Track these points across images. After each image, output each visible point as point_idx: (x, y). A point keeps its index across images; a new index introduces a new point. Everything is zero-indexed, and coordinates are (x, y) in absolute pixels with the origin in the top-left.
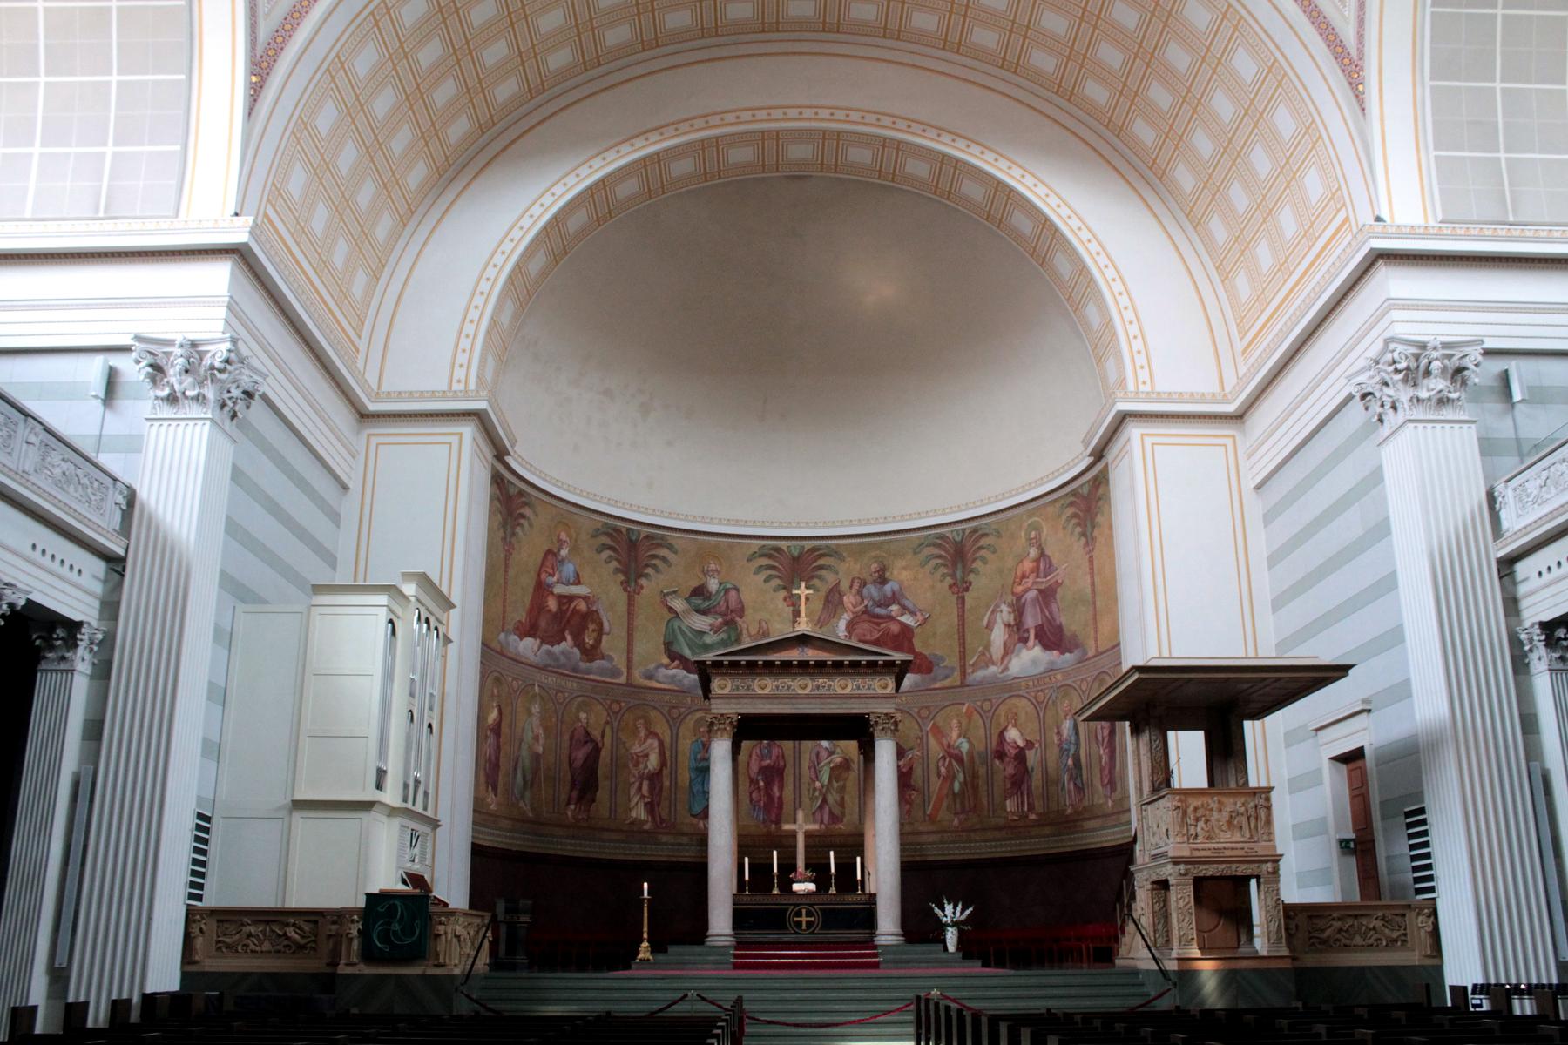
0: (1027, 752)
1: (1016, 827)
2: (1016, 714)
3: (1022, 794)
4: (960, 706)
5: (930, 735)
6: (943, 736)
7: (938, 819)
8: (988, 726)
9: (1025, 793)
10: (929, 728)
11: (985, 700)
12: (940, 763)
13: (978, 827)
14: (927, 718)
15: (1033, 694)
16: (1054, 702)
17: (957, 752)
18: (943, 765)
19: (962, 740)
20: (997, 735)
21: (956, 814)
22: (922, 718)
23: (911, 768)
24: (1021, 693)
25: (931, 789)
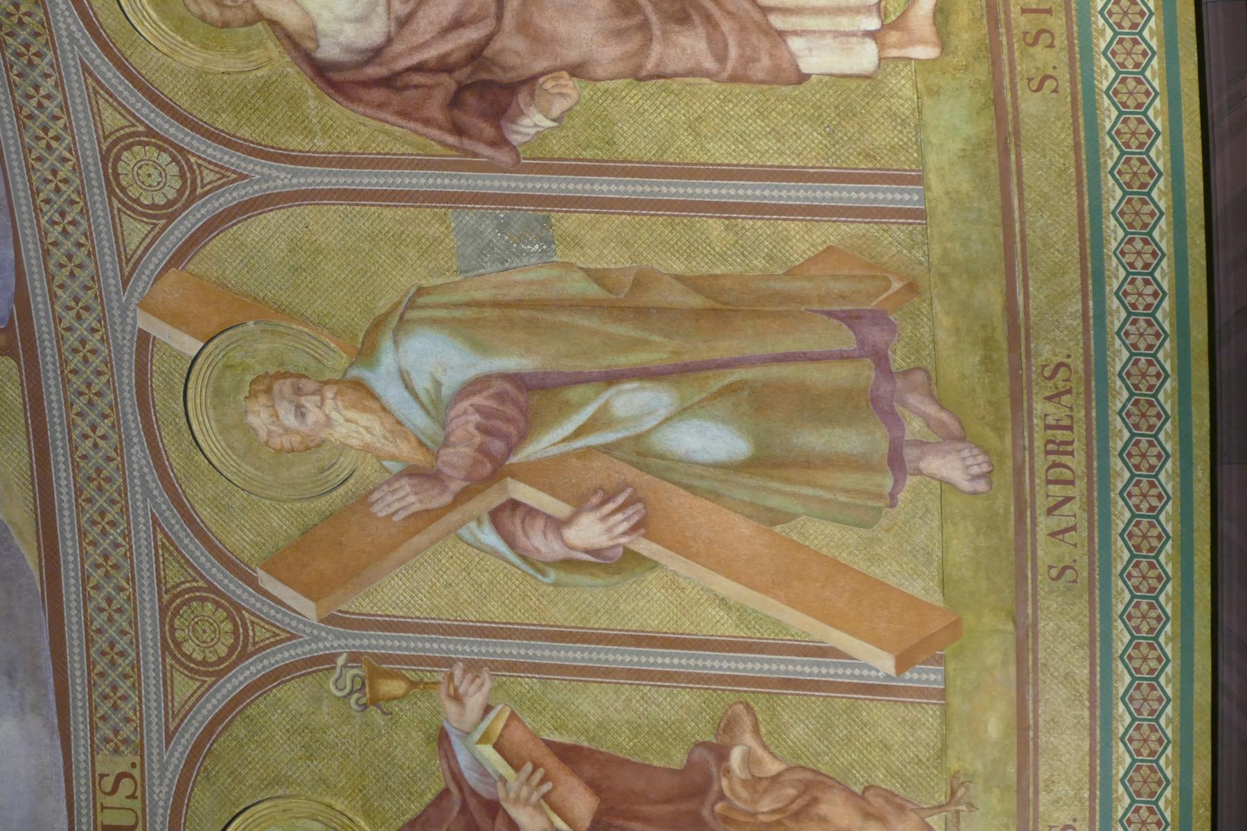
4: (157, 364)
5: (359, 604)
6: (363, 501)
7: (936, 599)
8: (282, 178)
10: (307, 608)
11: (112, 183)
12: (541, 542)
13: (991, 296)
14: (234, 610)
17: (466, 421)
18: (558, 525)
19: (383, 379)
20: (335, 109)
21: (896, 462)
22: (241, 651)
23: (568, 755)
25: (727, 628)
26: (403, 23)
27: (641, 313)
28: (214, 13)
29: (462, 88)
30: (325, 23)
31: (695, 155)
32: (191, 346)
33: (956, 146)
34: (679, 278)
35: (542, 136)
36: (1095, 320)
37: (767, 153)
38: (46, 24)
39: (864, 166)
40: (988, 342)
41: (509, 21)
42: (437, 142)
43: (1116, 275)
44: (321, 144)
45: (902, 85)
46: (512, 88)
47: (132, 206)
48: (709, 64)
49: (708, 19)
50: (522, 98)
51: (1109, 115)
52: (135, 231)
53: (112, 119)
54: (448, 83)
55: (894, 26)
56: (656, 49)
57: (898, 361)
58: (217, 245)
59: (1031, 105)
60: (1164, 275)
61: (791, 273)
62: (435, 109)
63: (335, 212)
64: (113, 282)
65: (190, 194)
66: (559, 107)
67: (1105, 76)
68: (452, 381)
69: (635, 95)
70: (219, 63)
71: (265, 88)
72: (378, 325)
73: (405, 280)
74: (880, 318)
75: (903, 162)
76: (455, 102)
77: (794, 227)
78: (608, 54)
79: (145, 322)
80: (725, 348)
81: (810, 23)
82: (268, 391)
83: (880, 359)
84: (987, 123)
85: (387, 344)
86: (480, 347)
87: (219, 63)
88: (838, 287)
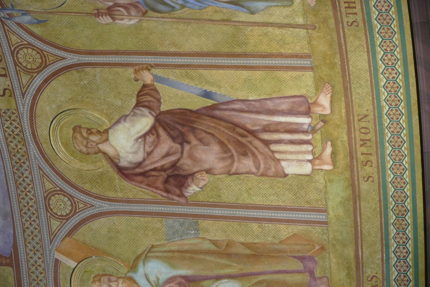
0: (164, 108)
1: (352, 155)
2: (77, 129)
3: (267, 129)
4: (61, 270)
8: (106, 207)
9: (265, 119)
11: (48, 207)
13: (350, 252)
15: (25, 79)
16: (39, 22)
19: (139, 277)
20: (126, 183)
24: (25, 111)
26: (149, 154)
27: (229, 256)
28: (84, 149)
29: (169, 177)
30: (122, 154)
31: (249, 201)
32: (73, 264)
33: (339, 200)
34: (243, 244)
35: (196, 194)
36: (386, 261)
37: (273, 201)
38: (27, 152)
39: (306, 206)
40: (349, 268)
41: (185, 154)
42: (160, 195)
43: (393, 245)
44: (120, 195)
45: (320, 179)
46: (186, 177)
47: (54, 216)
48: (254, 170)
49: (254, 154)
50: (189, 180)
51: (391, 190)
52: (55, 224)
53: (48, 185)
54: (164, 175)
55: (318, 158)
56: (236, 165)
57: (318, 274)
58: (83, 229)
59: (364, 186)
60: (410, 246)
61: (281, 242)
62: (159, 184)
63: (124, 218)
64: (47, 241)
65: (74, 211)
66: (202, 184)
67: (390, 177)
68: (163, 278)
69: (228, 180)
70: (86, 167)
71: (101, 175)
72: (138, 258)
73: (147, 242)
74: (311, 259)
75: (320, 205)
76: (166, 181)
77: (282, 227)
78: (219, 166)
79: (58, 256)
80: (257, 268)
81: (289, 157)
82: (99, 280)
83: (311, 273)
84: (349, 192)
85: (141, 264)
86: (173, 266)
87: (86, 167)
88: (297, 248)
